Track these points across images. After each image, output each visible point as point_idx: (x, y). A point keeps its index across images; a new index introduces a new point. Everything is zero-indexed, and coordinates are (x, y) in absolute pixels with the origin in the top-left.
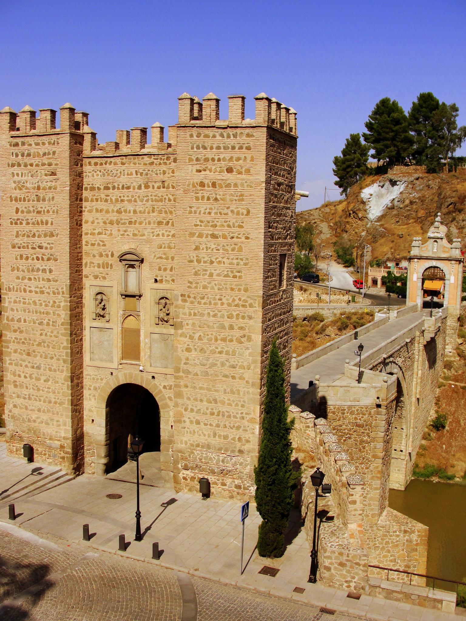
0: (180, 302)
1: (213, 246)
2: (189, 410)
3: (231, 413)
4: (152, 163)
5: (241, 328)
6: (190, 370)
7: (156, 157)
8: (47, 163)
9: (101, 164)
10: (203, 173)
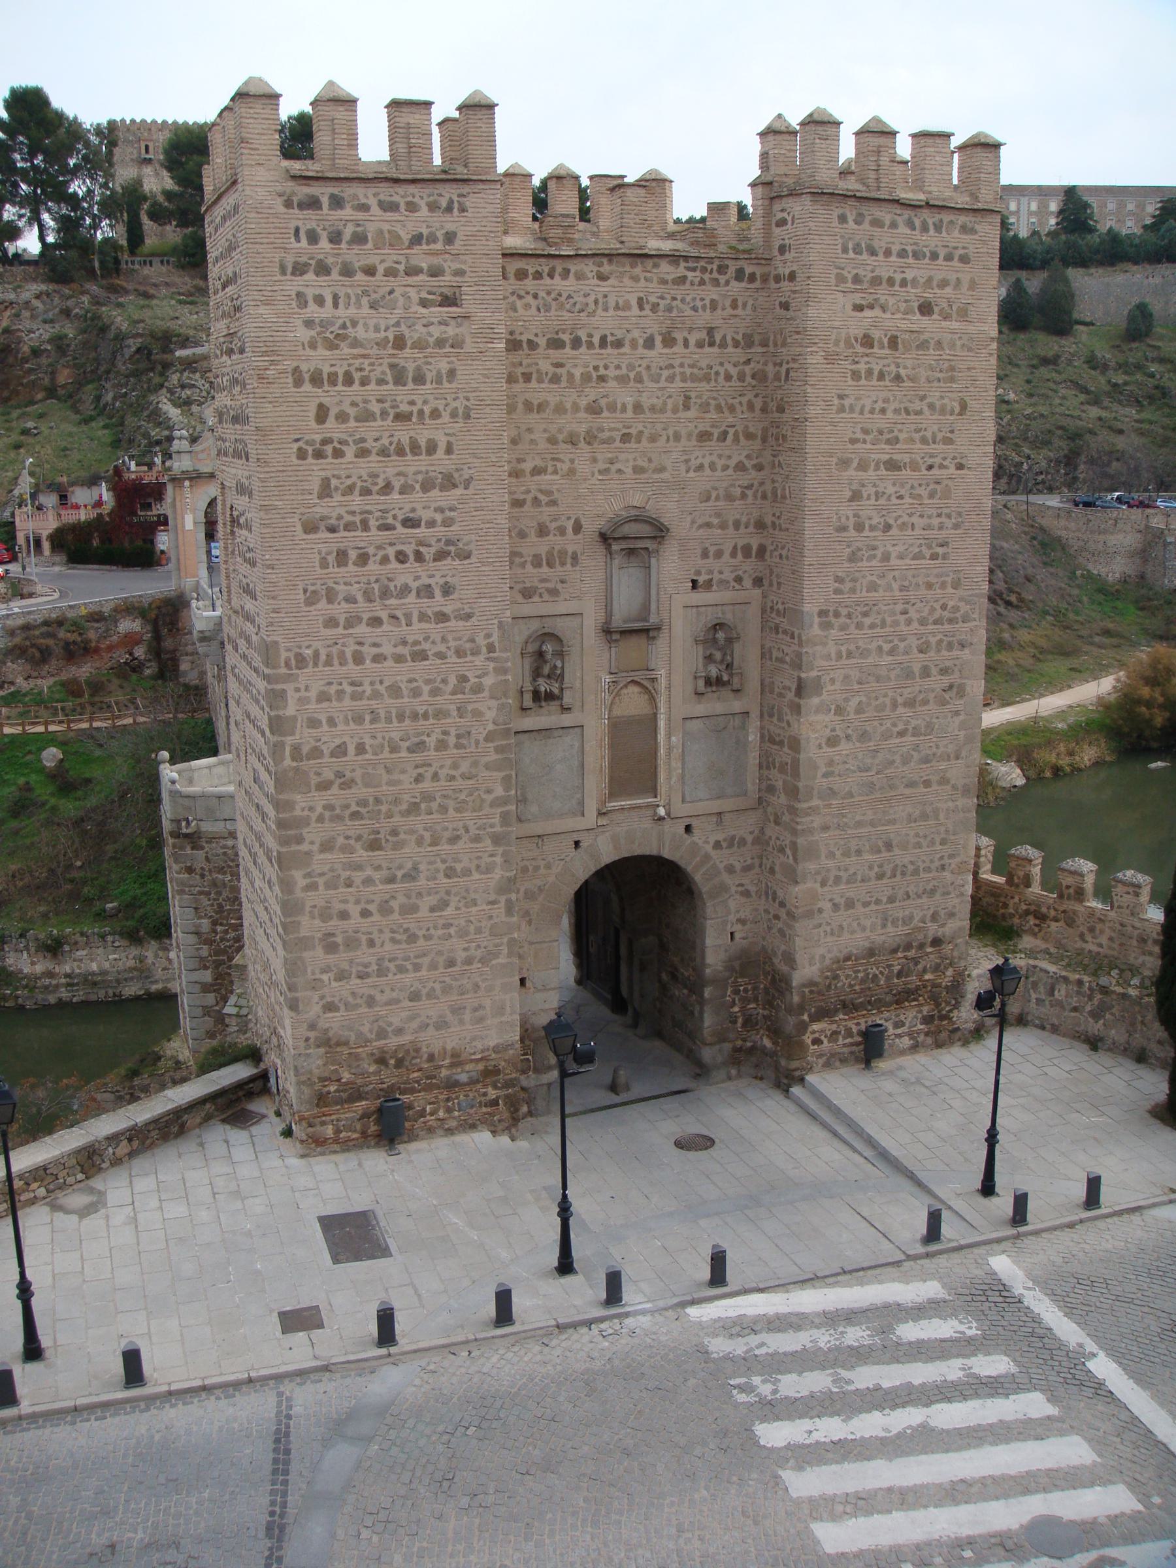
0: (816, 630)
1: (891, 490)
2: (830, 882)
3: (920, 864)
4: (682, 280)
5: (944, 671)
6: (835, 787)
7: (690, 264)
8: (424, 265)
9: (538, 276)
10: (867, 313)
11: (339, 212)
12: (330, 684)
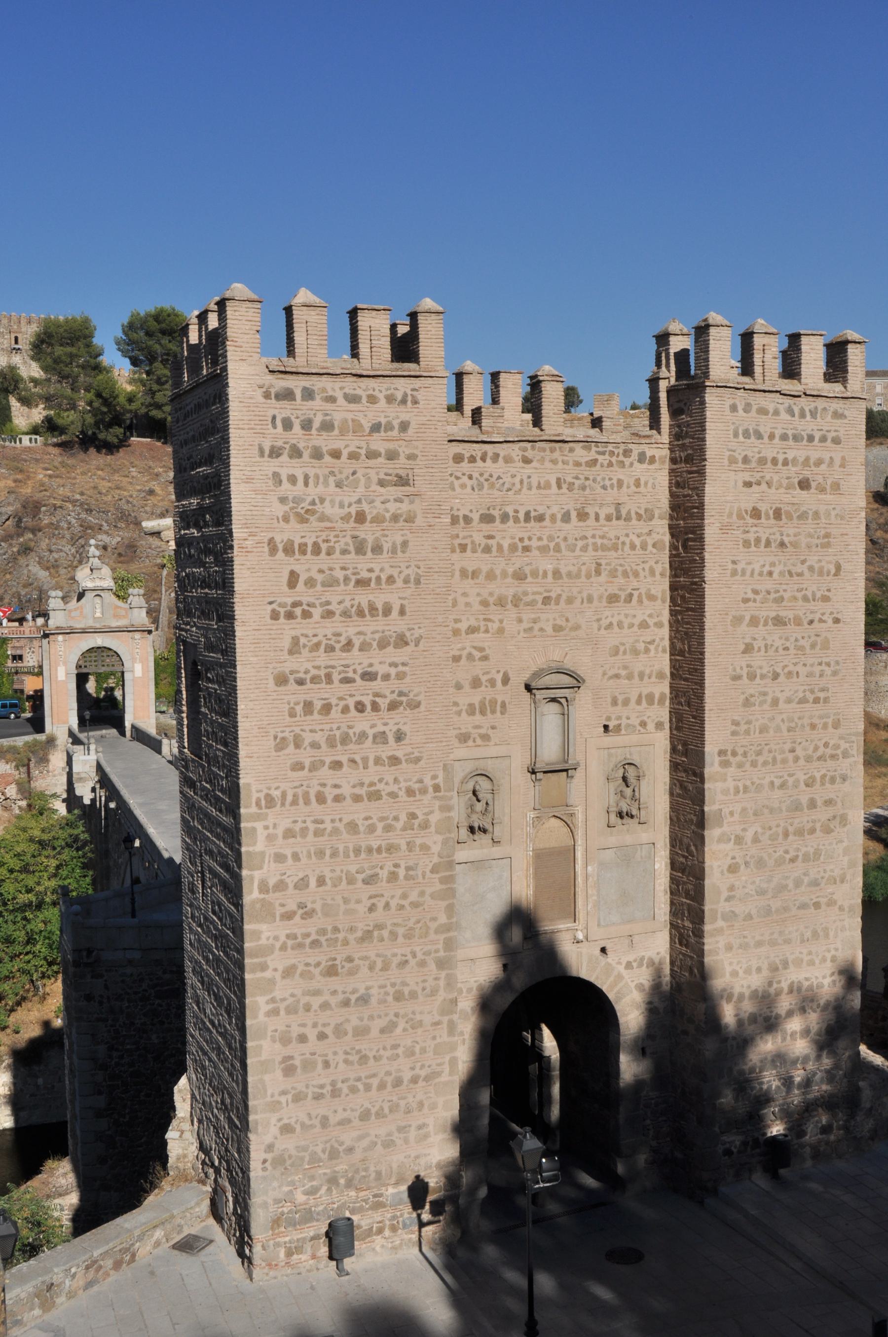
3: (814, 980)
5: (829, 802)
7: (600, 449)
8: (383, 451)
9: (472, 460)
10: (755, 488)
11: (310, 403)
12: (295, 822)
